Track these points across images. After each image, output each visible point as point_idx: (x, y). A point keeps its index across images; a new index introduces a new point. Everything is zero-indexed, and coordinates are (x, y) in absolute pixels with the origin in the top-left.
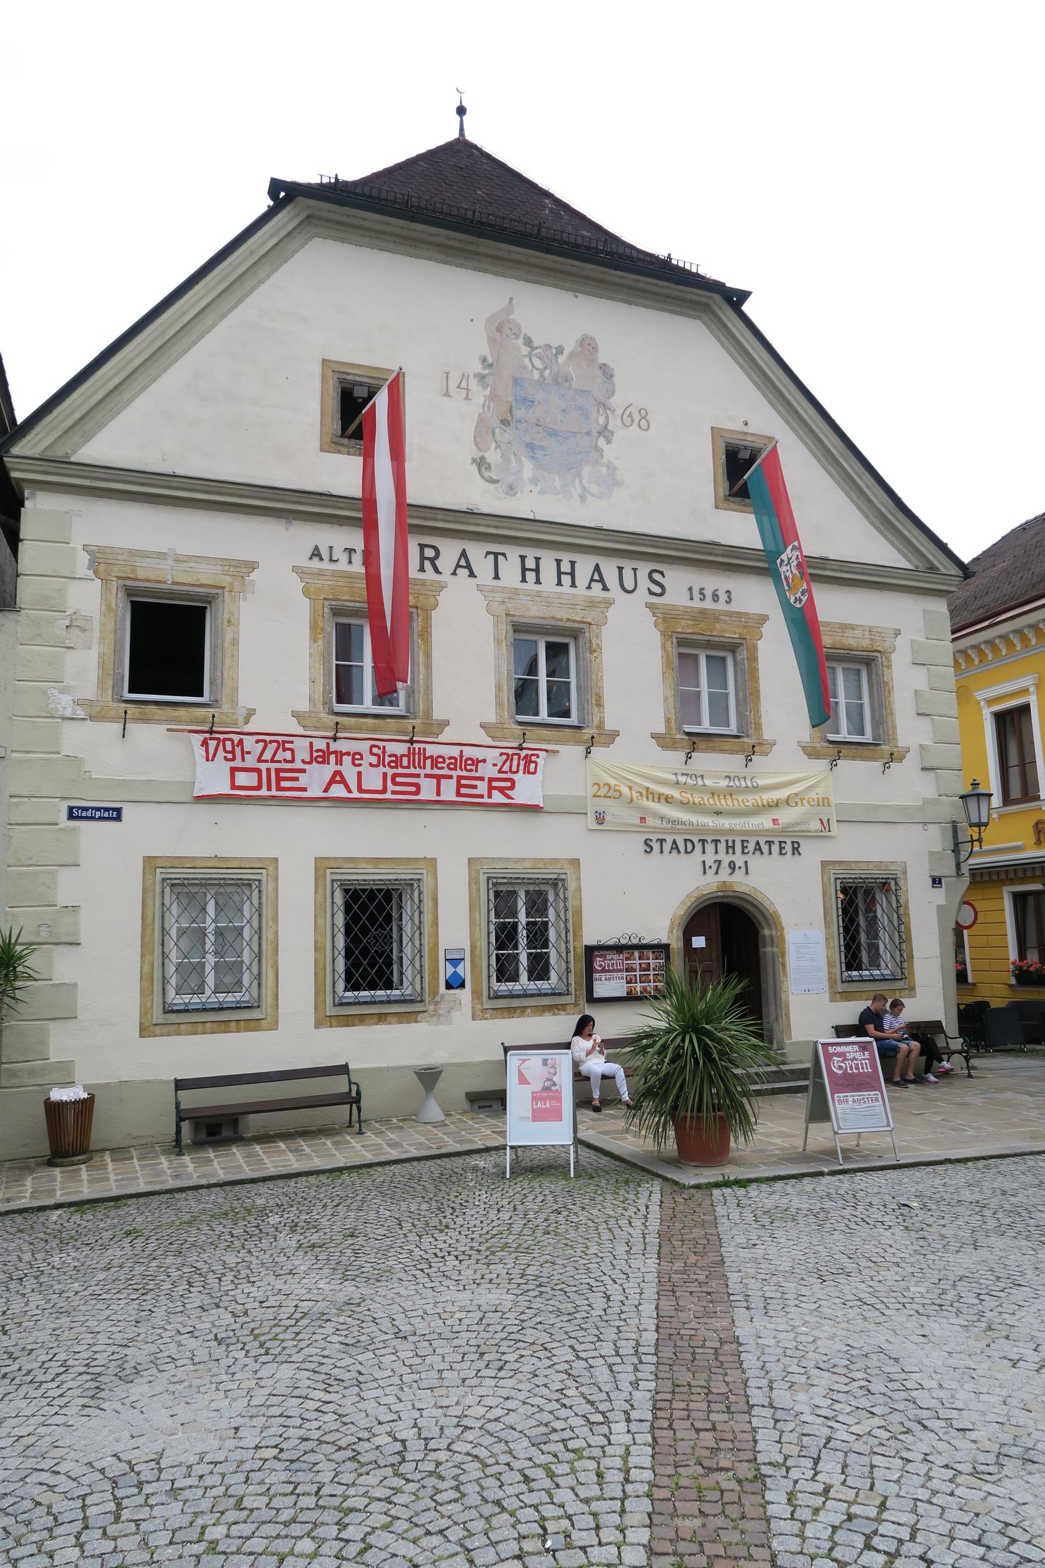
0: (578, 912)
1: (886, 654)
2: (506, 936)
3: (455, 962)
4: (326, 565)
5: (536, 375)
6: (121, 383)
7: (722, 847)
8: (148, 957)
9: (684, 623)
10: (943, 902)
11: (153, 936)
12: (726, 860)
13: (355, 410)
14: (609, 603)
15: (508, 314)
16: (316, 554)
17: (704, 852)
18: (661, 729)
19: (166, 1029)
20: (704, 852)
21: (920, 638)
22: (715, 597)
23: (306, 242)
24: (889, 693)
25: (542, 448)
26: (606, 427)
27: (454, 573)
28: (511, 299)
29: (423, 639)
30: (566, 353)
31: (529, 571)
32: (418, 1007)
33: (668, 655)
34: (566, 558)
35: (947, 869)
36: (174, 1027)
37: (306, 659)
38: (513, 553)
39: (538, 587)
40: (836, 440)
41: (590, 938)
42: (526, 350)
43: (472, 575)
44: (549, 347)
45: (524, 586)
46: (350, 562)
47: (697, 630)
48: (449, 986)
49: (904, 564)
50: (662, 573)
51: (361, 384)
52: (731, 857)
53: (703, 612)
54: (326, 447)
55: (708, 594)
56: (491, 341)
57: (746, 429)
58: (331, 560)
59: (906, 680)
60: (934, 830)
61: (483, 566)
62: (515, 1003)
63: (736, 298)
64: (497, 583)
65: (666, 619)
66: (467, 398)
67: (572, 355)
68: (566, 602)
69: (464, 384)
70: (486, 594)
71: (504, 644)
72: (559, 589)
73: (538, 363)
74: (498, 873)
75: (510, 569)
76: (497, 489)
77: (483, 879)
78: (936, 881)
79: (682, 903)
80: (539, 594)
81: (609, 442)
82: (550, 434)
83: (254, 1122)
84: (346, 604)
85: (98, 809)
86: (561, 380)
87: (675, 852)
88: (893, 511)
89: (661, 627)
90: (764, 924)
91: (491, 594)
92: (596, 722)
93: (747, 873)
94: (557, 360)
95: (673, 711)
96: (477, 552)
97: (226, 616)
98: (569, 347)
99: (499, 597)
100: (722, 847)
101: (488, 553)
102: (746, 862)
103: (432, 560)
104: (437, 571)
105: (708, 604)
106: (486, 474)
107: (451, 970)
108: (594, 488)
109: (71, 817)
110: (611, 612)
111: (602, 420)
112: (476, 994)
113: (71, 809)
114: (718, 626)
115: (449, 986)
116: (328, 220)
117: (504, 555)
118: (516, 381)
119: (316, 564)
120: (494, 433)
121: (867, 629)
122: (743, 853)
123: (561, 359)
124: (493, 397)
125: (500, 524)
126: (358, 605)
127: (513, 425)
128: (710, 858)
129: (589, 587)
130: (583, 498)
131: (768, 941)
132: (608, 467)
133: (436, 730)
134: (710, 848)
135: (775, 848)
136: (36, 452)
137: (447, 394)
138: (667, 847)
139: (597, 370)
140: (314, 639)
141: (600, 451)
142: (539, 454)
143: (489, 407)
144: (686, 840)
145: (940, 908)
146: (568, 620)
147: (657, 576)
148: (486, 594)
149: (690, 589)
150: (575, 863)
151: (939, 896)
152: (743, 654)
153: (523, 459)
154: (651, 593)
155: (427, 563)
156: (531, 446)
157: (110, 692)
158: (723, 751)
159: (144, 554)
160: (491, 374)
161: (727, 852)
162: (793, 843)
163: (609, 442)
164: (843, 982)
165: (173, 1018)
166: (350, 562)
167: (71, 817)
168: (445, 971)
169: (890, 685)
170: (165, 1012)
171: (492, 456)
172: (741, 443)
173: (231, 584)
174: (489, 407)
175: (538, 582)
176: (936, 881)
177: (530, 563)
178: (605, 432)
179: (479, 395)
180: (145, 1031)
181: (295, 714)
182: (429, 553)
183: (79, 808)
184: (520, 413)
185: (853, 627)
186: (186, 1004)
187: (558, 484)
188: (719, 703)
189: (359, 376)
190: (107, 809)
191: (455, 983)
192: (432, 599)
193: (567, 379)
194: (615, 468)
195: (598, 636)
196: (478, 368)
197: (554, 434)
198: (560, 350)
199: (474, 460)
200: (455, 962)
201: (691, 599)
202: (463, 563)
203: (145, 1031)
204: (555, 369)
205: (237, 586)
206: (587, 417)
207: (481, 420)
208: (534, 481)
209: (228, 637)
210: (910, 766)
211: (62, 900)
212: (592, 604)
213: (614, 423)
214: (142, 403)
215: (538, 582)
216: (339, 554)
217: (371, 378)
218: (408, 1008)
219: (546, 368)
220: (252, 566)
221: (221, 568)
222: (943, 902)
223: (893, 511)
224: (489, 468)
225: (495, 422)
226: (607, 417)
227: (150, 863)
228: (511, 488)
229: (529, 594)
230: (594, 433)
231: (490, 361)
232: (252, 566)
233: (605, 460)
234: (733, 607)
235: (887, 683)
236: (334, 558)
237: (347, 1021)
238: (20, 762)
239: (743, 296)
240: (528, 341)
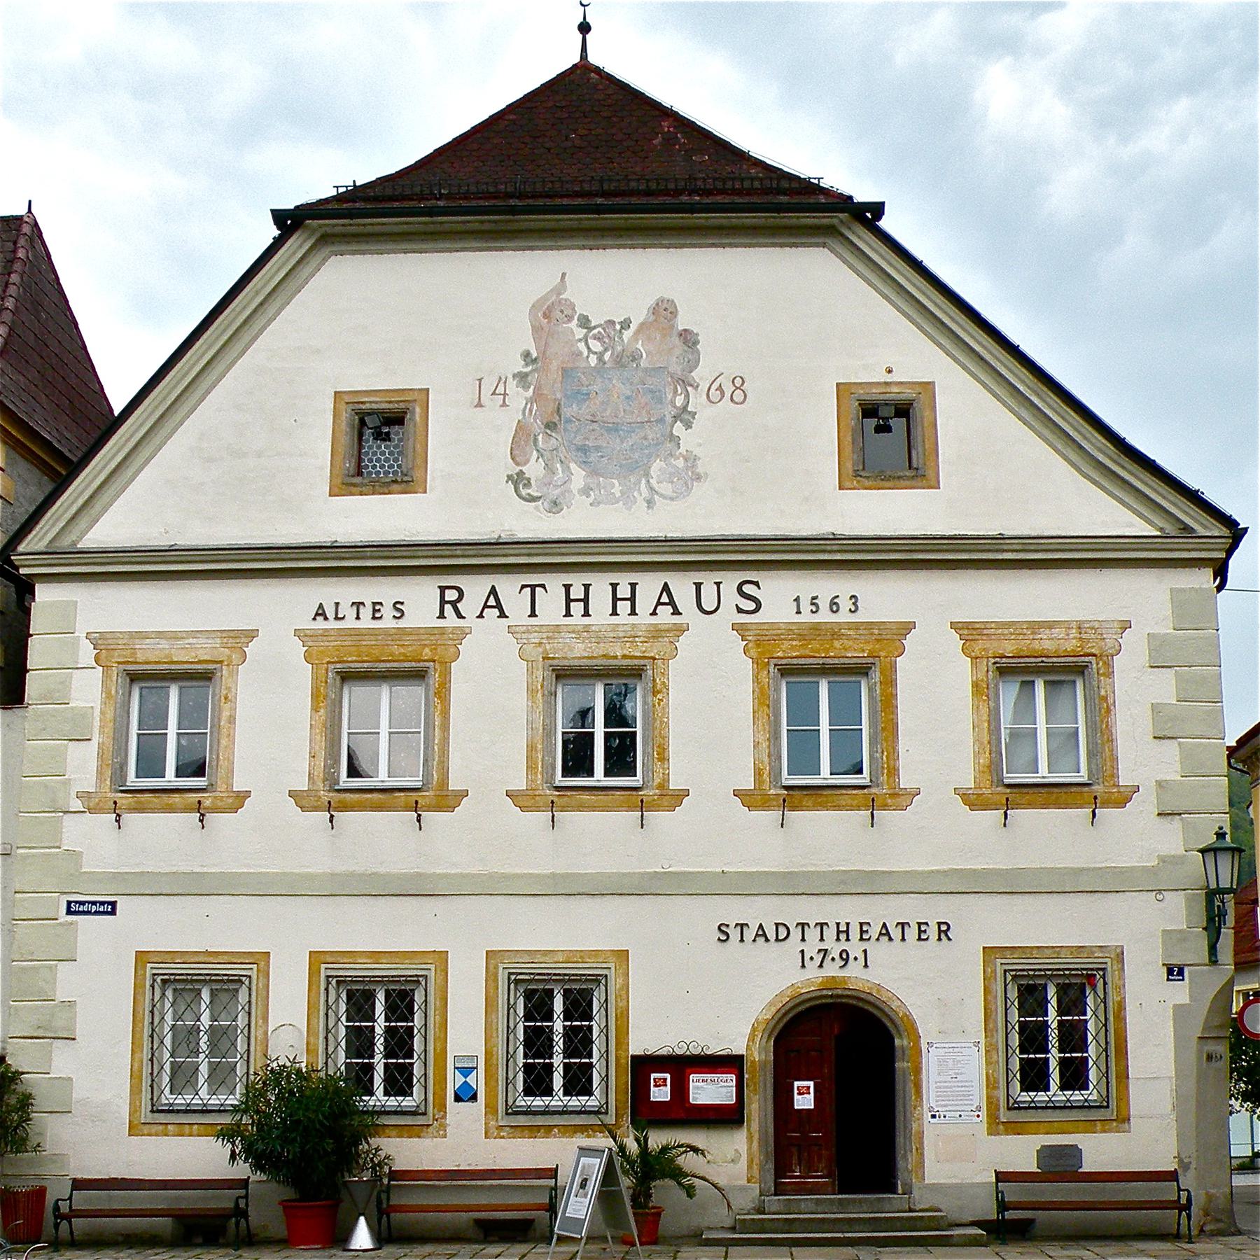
1: (1106, 659)
2: (537, 1042)
3: (466, 1072)
4: (332, 624)
5: (593, 360)
6: (125, 459)
7: (830, 933)
8: (137, 1056)
9: (786, 644)
10: (1186, 1000)
11: (146, 1030)
12: (835, 950)
13: (379, 436)
14: (681, 630)
15: (560, 294)
17: (803, 940)
19: (155, 1128)
20: (803, 940)
21: (1167, 629)
22: (834, 606)
23: (325, 260)
24: (1108, 711)
25: (598, 448)
26: (685, 408)
27: (481, 616)
28: (564, 275)
29: (440, 698)
30: (633, 327)
32: (420, 1120)
33: (762, 689)
34: (624, 581)
36: (161, 1127)
38: (555, 583)
39: (586, 620)
40: (1024, 373)
41: (637, 1047)
43: (503, 615)
44: (613, 323)
45: (568, 620)
46: (358, 618)
47: (807, 652)
48: (458, 1099)
49: (1138, 526)
50: (757, 584)
52: (844, 945)
53: (816, 627)
54: (336, 490)
55: (824, 604)
56: (537, 330)
57: (889, 378)
58: (337, 618)
62: (539, 1121)
64: (533, 621)
65: (761, 642)
66: (504, 404)
67: (642, 326)
68: (621, 635)
69: (501, 389)
70: (519, 636)
71: (540, 695)
72: (614, 619)
73: (596, 346)
74: (526, 967)
76: (536, 508)
77: (502, 977)
78: (1175, 972)
79: (771, 1004)
80: (587, 629)
81: (688, 426)
82: (609, 430)
83: (164, 1224)
84: (352, 665)
85: (94, 903)
87: (761, 940)
88: (1115, 457)
89: (753, 653)
90: (893, 1032)
91: (524, 636)
92: (657, 781)
93: (866, 966)
94: (621, 338)
95: (766, 759)
96: (509, 587)
97: (224, 692)
100: (830, 933)
101: (523, 587)
102: (865, 951)
103: (454, 604)
104: (460, 616)
105: (825, 616)
106: (524, 492)
107: (460, 1080)
108: (666, 488)
109: (69, 912)
111: (679, 401)
112: (491, 1108)
113: (69, 903)
114: (837, 644)
115: (458, 1099)
116: (344, 235)
117: (543, 586)
118: (566, 372)
119: (320, 624)
120: (536, 440)
121: (1074, 625)
122: (861, 939)
123: (627, 334)
124: (538, 397)
125: (532, 551)
126: (365, 665)
127: (561, 427)
129: (654, 613)
130: (650, 503)
131: (898, 1054)
132: (686, 460)
133: (452, 803)
134: (813, 934)
135: (912, 933)
136: (41, 546)
137: (479, 405)
138: (750, 934)
139: (676, 340)
140: (315, 709)
141: (676, 441)
142: (593, 457)
143: (531, 411)
144: (777, 925)
145: (1178, 1008)
146: (624, 657)
147: (748, 589)
148: (519, 636)
149: (797, 600)
150: (623, 956)
151: (1180, 993)
153: (573, 465)
154: (740, 611)
155: (448, 607)
156: (583, 450)
157: (108, 783)
158: (838, 808)
159: (143, 635)
160: (533, 370)
161: (838, 939)
162: (939, 924)
163: (688, 426)
164: (1009, 1109)
165: (162, 1118)
166: (358, 618)
167: (69, 912)
168: (454, 1081)
169: (1110, 701)
170: (152, 1111)
171: (534, 469)
172: (882, 397)
173: (229, 657)
174: (531, 411)
175: (586, 614)
176: (1175, 972)
177: (577, 592)
178: (684, 416)
179: (519, 397)
180: (134, 1130)
181: (292, 794)
182: (451, 595)
183: (76, 902)
185: (1050, 625)
186: (171, 1105)
187: (617, 490)
188: (845, 740)
189: (376, 402)
190: (102, 903)
191: (466, 1095)
192: (452, 650)
193: (635, 357)
194: (696, 458)
195: (665, 674)
196: (520, 366)
197: (614, 429)
198: (626, 324)
199: (509, 477)
200: (466, 1072)
201: (799, 612)
202: (492, 602)
203: (134, 1130)
204: (619, 348)
205: (236, 657)
206: (660, 401)
207: (520, 426)
208: (586, 491)
209: (226, 714)
210: (1144, 806)
211: (61, 996)
212: (656, 633)
213: (697, 401)
214: (147, 475)
215: (586, 614)
216: (346, 610)
217: (390, 402)
218: (409, 1120)
219: (606, 350)
220: (252, 635)
221: (218, 641)
222: (1186, 1000)
223: (1115, 457)
224: (528, 484)
225: (537, 426)
226: (687, 396)
228: (555, 503)
230: (669, 419)
231: (535, 355)
232: (252, 635)
233: (682, 450)
235: (1105, 698)
236: (340, 616)
238: (27, 856)
239: (878, 209)
240: (585, 322)
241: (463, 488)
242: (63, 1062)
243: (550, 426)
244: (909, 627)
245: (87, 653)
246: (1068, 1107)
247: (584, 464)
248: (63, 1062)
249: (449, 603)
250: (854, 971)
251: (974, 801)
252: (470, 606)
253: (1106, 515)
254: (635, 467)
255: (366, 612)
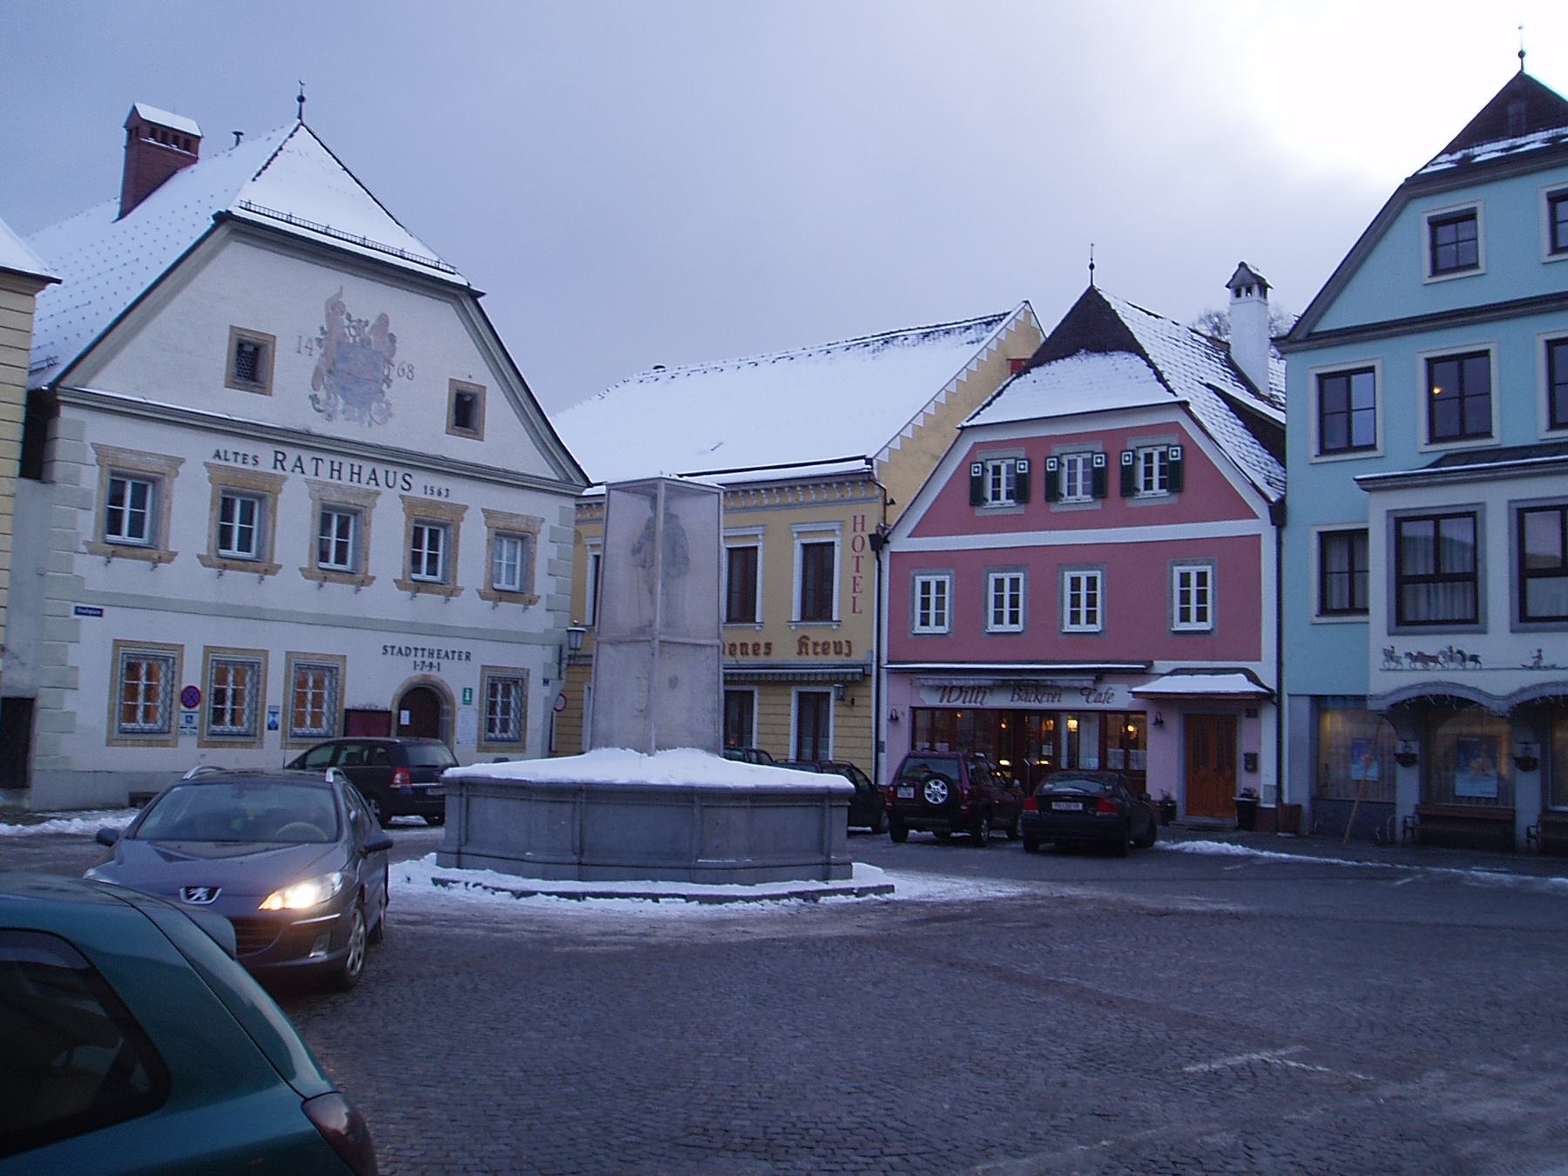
0: (343, 689)
1: (534, 534)
2: (300, 700)
3: (274, 714)
12: (428, 661)
14: (378, 494)
16: (218, 455)
18: (400, 577)
21: (556, 525)
22: (440, 493)
31: (336, 471)
34: (357, 462)
35: (553, 674)
37: (207, 523)
38: (327, 458)
41: (347, 705)
42: (346, 322)
51: (249, 343)
53: (432, 502)
56: (328, 316)
59: (545, 551)
60: (549, 649)
61: (309, 466)
63: (475, 296)
65: (410, 504)
75: (325, 469)
86: (366, 343)
96: (307, 457)
98: (372, 322)
99: (317, 487)
105: (435, 498)
109: (77, 613)
110: (379, 501)
112: (284, 735)
118: (338, 343)
119: (217, 461)
128: (419, 660)
151: (546, 691)
152: (451, 530)
156: (343, 388)
159: (123, 451)
168: (268, 719)
171: (322, 394)
176: (546, 682)
178: (387, 380)
179: (318, 352)
180: (109, 743)
181: (199, 556)
184: (340, 366)
196: (318, 334)
200: (274, 714)
203: (109, 743)
208: (344, 412)
213: (393, 375)
220: (182, 461)
225: (324, 369)
227: (117, 643)
229: (333, 485)
232: (182, 461)
234: (448, 500)
237: (214, 745)
240: (349, 317)
241: (288, 399)
242: (70, 702)
243: (330, 372)
244: (466, 508)
245: (91, 456)
246: (503, 740)
247: (344, 397)
248: (70, 702)
249: (279, 462)
250: (434, 672)
251: (484, 597)
252: (288, 464)
253: (538, 466)
254: (365, 404)
255: (240, 458)
